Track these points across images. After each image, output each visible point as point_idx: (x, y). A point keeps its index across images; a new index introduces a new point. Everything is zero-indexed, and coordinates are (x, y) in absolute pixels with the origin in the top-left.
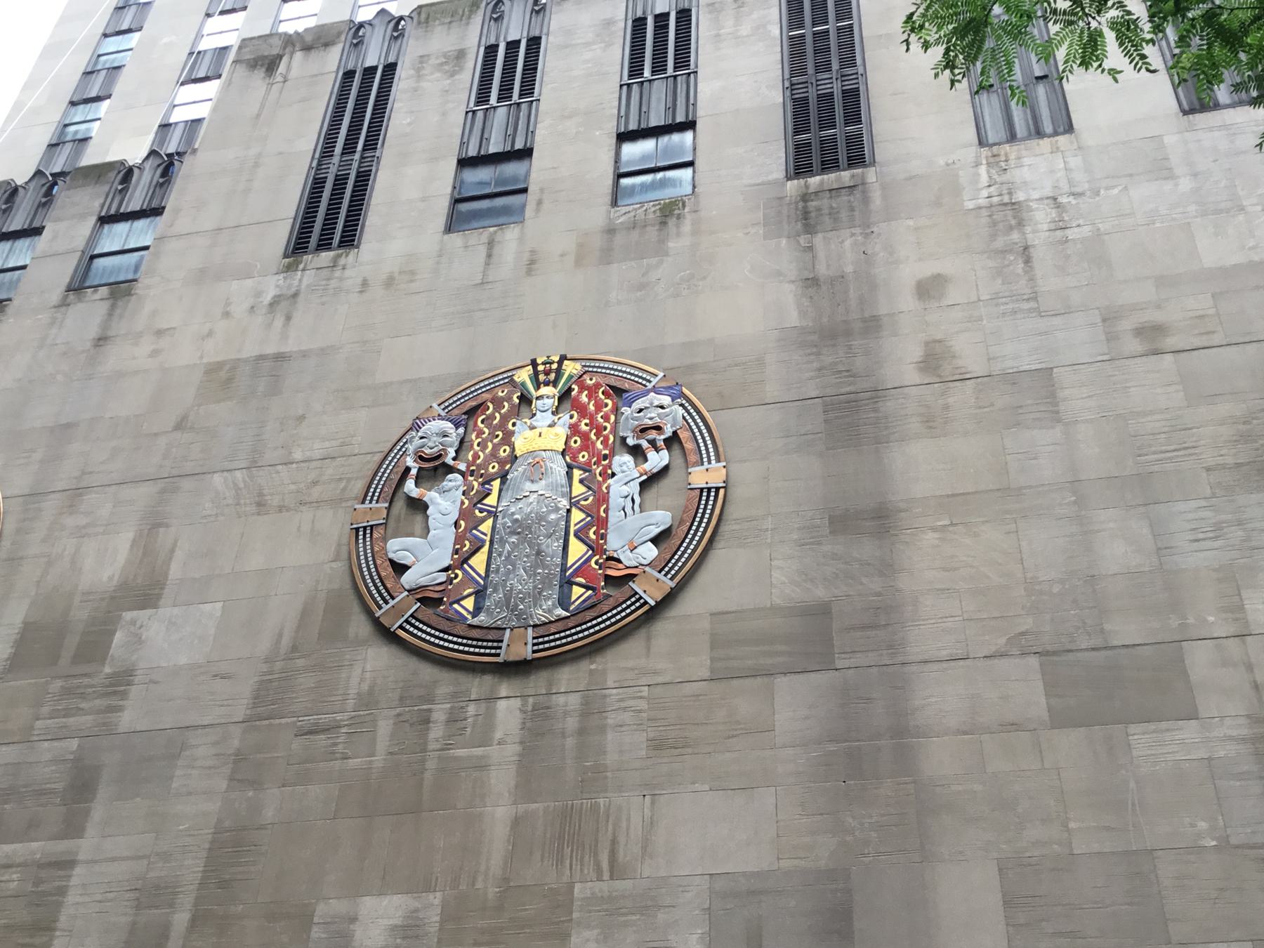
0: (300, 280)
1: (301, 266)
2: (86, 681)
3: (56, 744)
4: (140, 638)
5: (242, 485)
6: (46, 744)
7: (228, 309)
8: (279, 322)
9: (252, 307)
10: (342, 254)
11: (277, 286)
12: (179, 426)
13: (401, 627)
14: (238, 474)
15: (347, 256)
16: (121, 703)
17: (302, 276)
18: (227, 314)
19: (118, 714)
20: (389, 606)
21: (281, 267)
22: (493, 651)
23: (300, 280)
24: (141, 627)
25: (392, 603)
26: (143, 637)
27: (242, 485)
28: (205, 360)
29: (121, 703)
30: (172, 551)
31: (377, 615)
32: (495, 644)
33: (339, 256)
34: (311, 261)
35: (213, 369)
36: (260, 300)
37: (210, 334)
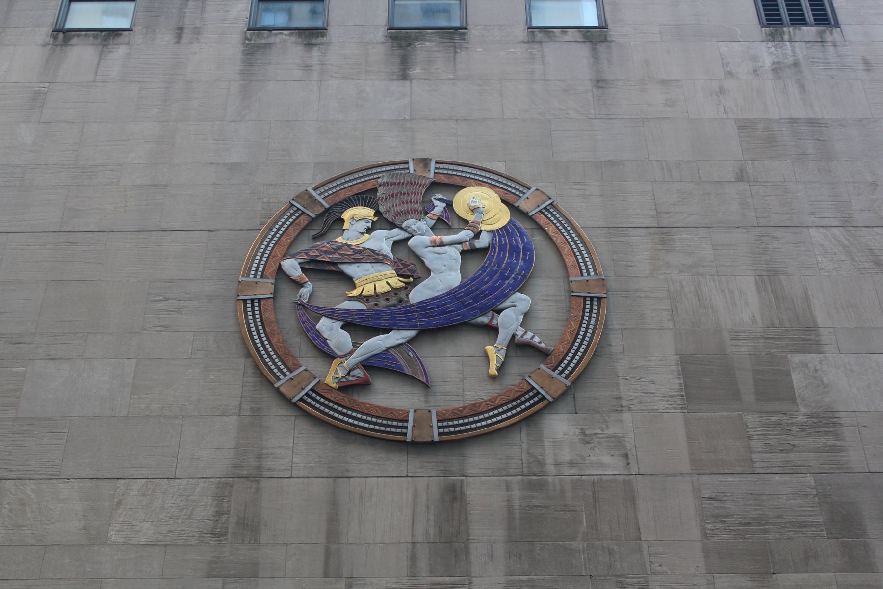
0: (793, 51)
1: (786, 37)
2: (785, 418)
3: (787, 478)
4: (822, 381)
5: (846, 243)
6: (777, 477)
7: (728, 69)
8: (794, 89)
9: (755, 71)
10: (824, 31)
11: (771, 53)
12: (741, 176)
13: (301, 399)
14: (835, 230)
15: (831, 34)
16: (838, 443)
17: (793, 47)
18: (730, 74)
19: (842, 454)
20: (287, 378)
21: (764, 35)
22: (399, 430)
23: (793, 51)
24: (816, 371)
25: (290, 375)
26: (825, 381)
27: (846, 243)
28: (731, 116)
29: (838, 443)
30: (807, 298)
31: (276, 385)
32: (400, 424)
33: (823, 32)
34: (794, 35)
35: (746, 126)
36: (760, 64)
37: (722, 91)
